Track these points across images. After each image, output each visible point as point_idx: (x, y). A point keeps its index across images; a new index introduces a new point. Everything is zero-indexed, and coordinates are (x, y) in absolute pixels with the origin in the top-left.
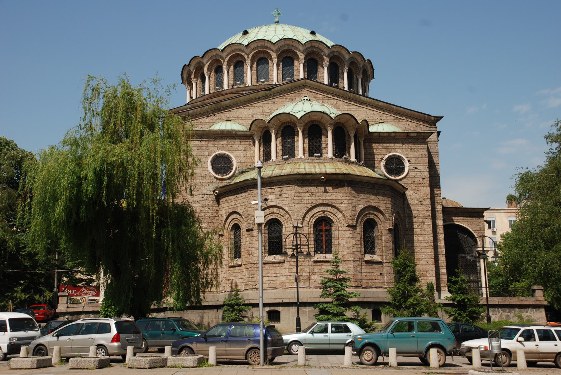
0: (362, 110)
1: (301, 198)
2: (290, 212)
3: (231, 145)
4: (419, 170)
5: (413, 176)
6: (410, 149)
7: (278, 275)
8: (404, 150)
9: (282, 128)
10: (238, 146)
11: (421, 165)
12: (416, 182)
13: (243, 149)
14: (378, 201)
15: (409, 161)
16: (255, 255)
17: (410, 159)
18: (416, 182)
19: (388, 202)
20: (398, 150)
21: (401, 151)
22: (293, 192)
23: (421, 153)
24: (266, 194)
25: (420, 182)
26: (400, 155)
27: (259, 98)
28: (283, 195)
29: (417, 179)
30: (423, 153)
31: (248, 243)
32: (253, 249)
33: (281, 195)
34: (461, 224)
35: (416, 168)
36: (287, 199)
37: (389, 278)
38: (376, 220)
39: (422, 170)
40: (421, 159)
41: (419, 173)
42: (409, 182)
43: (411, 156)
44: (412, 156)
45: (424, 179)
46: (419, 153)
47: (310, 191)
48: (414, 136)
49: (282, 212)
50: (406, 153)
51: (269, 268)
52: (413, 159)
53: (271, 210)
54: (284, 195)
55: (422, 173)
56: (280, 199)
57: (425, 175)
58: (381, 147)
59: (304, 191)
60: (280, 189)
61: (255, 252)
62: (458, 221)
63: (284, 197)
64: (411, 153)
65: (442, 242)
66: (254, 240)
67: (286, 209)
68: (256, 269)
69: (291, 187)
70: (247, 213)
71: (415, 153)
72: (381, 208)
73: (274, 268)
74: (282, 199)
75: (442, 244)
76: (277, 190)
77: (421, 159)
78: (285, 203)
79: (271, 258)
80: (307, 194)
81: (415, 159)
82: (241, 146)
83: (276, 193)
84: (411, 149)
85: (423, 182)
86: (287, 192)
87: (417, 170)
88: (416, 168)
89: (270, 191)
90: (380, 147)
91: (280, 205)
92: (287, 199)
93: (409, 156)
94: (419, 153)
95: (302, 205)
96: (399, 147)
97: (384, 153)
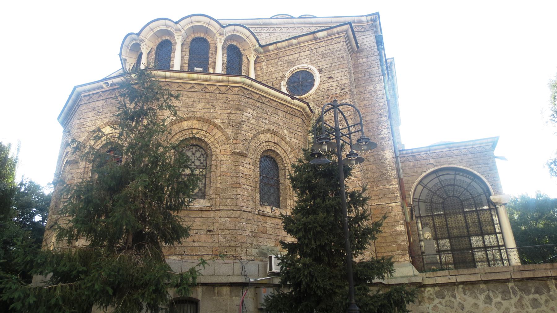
0: (275, 35)
1: (82, 121)
4: (335, 80)
5: (326, 89)
6: (320, 56)
8: (313, 59)
11: (338, 71)
12: (331, 97)
14: (212, 111)
15: (320, 71)
17: (321, 68)
18: (331, 97)
19: (233, 112)
20: (305, 61)
21: (309, 61)
23: (337, 56)
25: (337, 95)
26: (305, 65)
29: (333, 92)
30: (340, 56)
34: (459, 167)
35: (330, 78)
37: (228, 237)
38: (206, 140)
39: (339, 79)
40: (338, 63)
41: (335, 83)
42: (320, 99)
43: (324, 64)
44: (323, 63)
45: (343, 89)
46: (334, 57)
47: (97, 109)
48: (325, 37)
50: (315, 62)
52: (326, 66)
55: (340, 82)
57: (344, 85)
58: (282, 63)
59: (89, 110)
62: (454, 162)
64: (323, 60)
65: (393, 183)
71: (328, 58)
72: (218, 121)
75: (394, 186)
77: (338, 63)
80: (91, 114)
81: (328, 66)
84: (323, 55)
85: (341, 94)
87: (332, 80)
88: (330, 78)
90: (279, 63)
93: (320, 64)
94: (334, 57)
95: (83, 130)
96: (305, 57)
97: (285, 69)
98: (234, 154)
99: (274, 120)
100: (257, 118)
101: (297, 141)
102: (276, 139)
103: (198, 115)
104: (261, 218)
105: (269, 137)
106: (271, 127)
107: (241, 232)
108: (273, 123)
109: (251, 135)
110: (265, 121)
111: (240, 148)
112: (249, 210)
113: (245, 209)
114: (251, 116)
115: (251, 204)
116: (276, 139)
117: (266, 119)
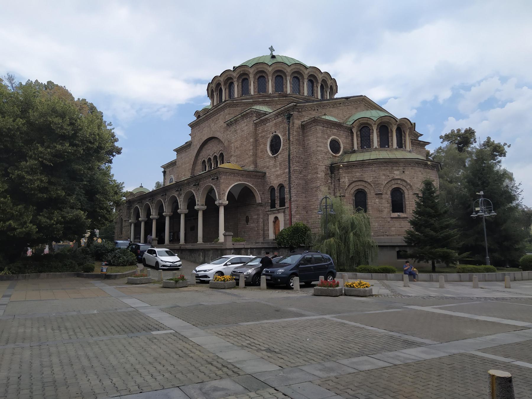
2: (411, 184)
3: (339, 133)
7: (403, 226)
9: (380, 126)
10: (342, 134)
13: (345, 137)
16: (385, 212)
22: (413, 170)
24: (392, 170)
27: (340, 103)
28: (405, 172)
31: (377, 203)
32: (383, 207)
33: (404, 172)
36: (409, 175)
49: (404, 184)
51: (395, 221)
53: (396, 181)
54: (406, 173)
56: (403, 175)
60: (403, 168)
61: (384, 209)
63: (406, 173)
66: (383, 201)
67: (408, 181)
68: (385, 221)
69: (411, 167)
70: (377, 182)
73: (399, 221)
74: (405, 175)
76: (401, 168)
78: (407, 178)
79: (396, 215)
82: (344, 134)
83: (400, 170)
86: (408, 170)
89: (395, 168)
91: (404, 178)
92: (409, 175)
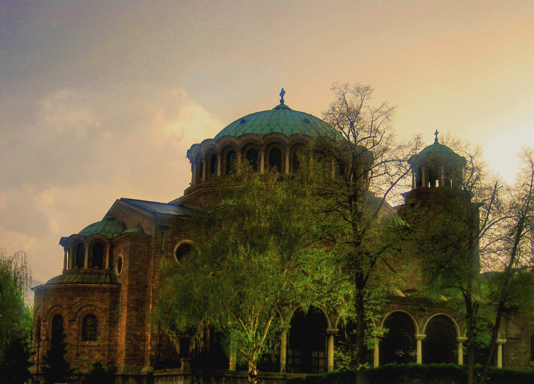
72: (64, 306)
98: (69, 321)
99: (91, 298)
100: (81, 301)
101: (105, 306)
102: (93, 308)
103: (58, 304)
104: (82, 347)
105: (88, 308)
106: (89, 303)
107: (71, 354)
108: (90, 301)
109: (77, 310)
110: (85, 301)
111: (71, 318)
112: (75, 344)
113: (73, 344)
114: (77, 300)
115: (76, 342)
116: (93, 308)
117: (86, 299)
